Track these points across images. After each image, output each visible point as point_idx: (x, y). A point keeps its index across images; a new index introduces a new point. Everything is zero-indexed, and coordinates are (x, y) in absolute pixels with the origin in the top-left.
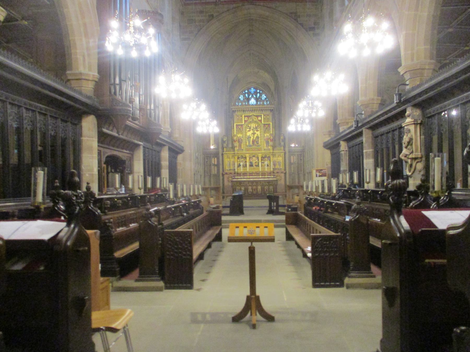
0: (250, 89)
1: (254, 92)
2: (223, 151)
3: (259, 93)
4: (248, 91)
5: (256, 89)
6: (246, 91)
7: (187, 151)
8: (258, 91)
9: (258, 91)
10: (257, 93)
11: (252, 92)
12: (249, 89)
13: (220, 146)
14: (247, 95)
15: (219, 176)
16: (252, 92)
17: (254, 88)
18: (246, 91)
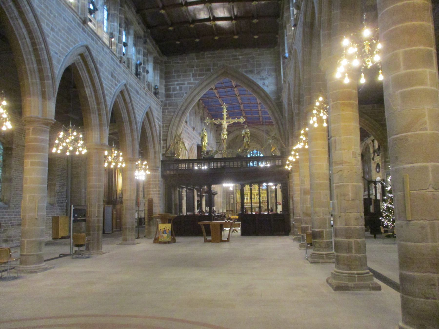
0: (254, 151)
1: (256, 153)
2: (236, 191)
3: (259, 153)
4: (252, 152)
5: (257, 151)
6: (251, 152)
7: (219, 193)
8: (258, 152)
9: (258, 152)
10: (258, 153)
11: (255, 153)
12: (253, 151)
13: (235, 189)
14: (252, 155)
15: (234, 204)
16: (255, 153)
17: (256, 151)
18: (251, 152)
